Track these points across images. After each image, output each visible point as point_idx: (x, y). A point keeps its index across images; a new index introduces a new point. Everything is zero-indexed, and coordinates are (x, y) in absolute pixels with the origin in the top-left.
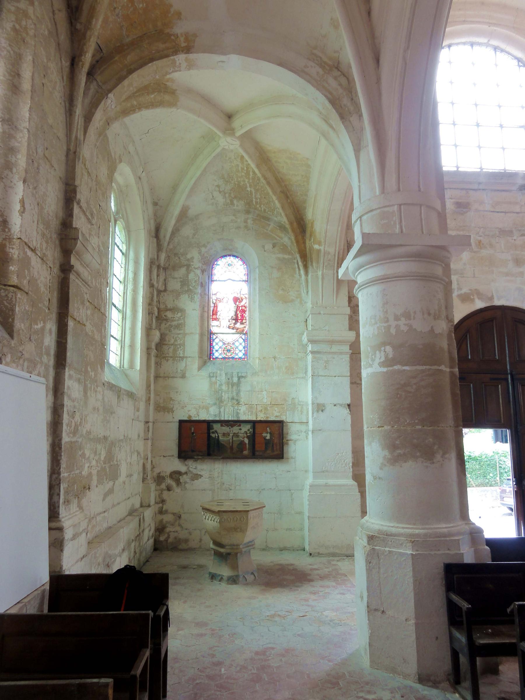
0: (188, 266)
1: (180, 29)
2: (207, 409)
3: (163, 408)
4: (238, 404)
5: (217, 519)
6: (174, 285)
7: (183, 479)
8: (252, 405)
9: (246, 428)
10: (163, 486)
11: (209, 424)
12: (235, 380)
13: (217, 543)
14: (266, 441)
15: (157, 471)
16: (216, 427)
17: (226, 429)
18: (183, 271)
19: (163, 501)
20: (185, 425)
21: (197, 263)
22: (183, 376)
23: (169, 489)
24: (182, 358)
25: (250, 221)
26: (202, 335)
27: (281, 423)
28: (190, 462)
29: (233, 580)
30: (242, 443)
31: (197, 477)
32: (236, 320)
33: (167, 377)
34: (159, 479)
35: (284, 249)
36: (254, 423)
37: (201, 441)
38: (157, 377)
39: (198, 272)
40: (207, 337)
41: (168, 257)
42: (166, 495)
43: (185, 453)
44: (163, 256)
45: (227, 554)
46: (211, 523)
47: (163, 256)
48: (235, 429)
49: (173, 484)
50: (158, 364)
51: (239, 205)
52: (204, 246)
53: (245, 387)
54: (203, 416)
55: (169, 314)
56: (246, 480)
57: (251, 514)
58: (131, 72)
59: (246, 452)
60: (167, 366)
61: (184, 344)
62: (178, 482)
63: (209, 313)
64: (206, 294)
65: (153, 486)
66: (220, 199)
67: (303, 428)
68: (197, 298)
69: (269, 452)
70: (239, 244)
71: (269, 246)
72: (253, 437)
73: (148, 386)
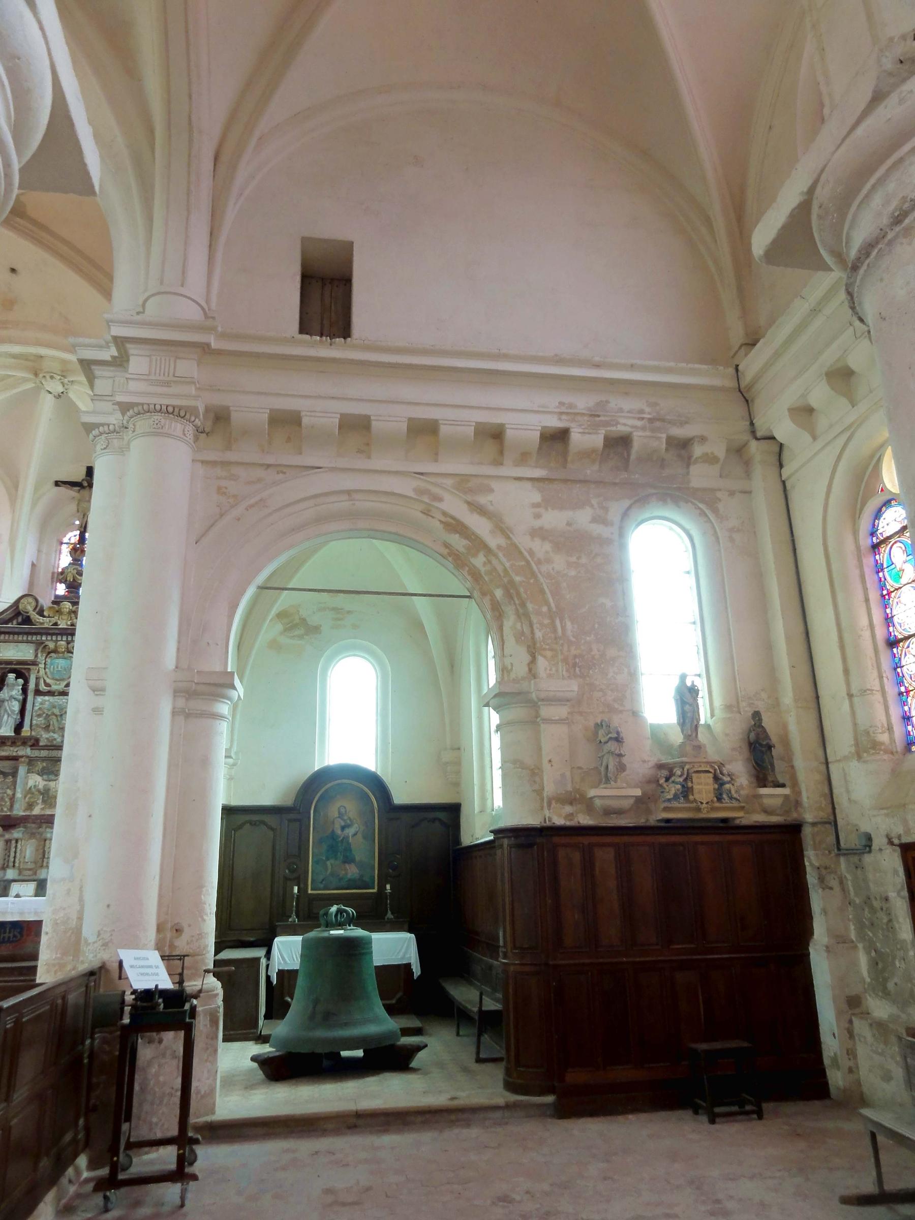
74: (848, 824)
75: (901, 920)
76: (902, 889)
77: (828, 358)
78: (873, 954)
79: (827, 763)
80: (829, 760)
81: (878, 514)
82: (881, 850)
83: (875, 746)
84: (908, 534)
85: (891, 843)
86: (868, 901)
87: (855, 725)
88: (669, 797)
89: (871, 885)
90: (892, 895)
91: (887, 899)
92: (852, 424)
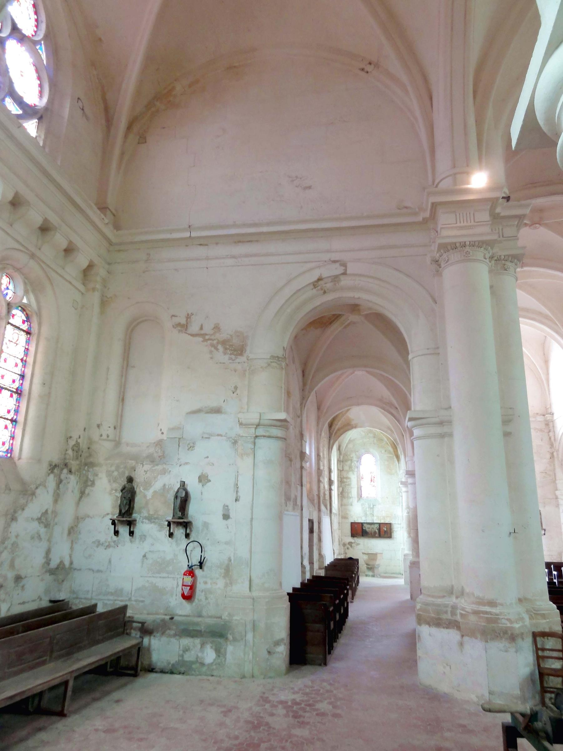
0: (351, 460)
1: (353, 423)
2: (361, 517)
3: (344, 517)
4: (373, 515)
5: (367, 556)
6: (346, 468)
7: (353, 545)
8: (378, 517)
9: (377, 526)
10: (346, 547)
11: (362, 524)
12: (372, 506)
13: (367, 564)
14: (384, 531)
15: (343, 541)
16: (365, 525)
17: (369, 526)
18: (349, 462)
19: (346, 553)
20: (353, 524)
21: (355, 459)
22: (352, 505)
23: (348, 548)
24: (351, 498)
25: (375, 441)
26: (358, 488)
27: (390, 524)
28: (355, 538)
29: (373, 576)
30: (375, 532)
31: (358, 544)
32: (371, 481)
33: (345, 505)
34: (344, 545)
35: (390, 453)
36: (380, 524)
37: (359, 530)
38: (341, 505)
39: (356, 462)
40: (360, 488)
41: (343, 457)
42: (347, 551)
43: (353, 535)
44: (342, 457)
45: (371, 568)
46: (366, 557)
47: (342, 457)
48: (372, 526)
49: (349, 547)
50: (342, 500)
51: (371, 435)
52: (358, 452)
53: (376, 509)
54: (360, 521)
55: (345, 480)
56: (377, 545)
57: (378, 555)
58: (341, 434)
59: (377, 535)
60: (345, 501)
61: (351, 492)
62: (351, 546)
63: (360, 478)
64: (358, 471)
65: (342, 547)
66: (363, 434)
67: (399, 526)
68: (355, 473)
69: (386, 535)
70: (371, 450)
71: (383, 451)
72: (379, 530)
73: (339, 509)
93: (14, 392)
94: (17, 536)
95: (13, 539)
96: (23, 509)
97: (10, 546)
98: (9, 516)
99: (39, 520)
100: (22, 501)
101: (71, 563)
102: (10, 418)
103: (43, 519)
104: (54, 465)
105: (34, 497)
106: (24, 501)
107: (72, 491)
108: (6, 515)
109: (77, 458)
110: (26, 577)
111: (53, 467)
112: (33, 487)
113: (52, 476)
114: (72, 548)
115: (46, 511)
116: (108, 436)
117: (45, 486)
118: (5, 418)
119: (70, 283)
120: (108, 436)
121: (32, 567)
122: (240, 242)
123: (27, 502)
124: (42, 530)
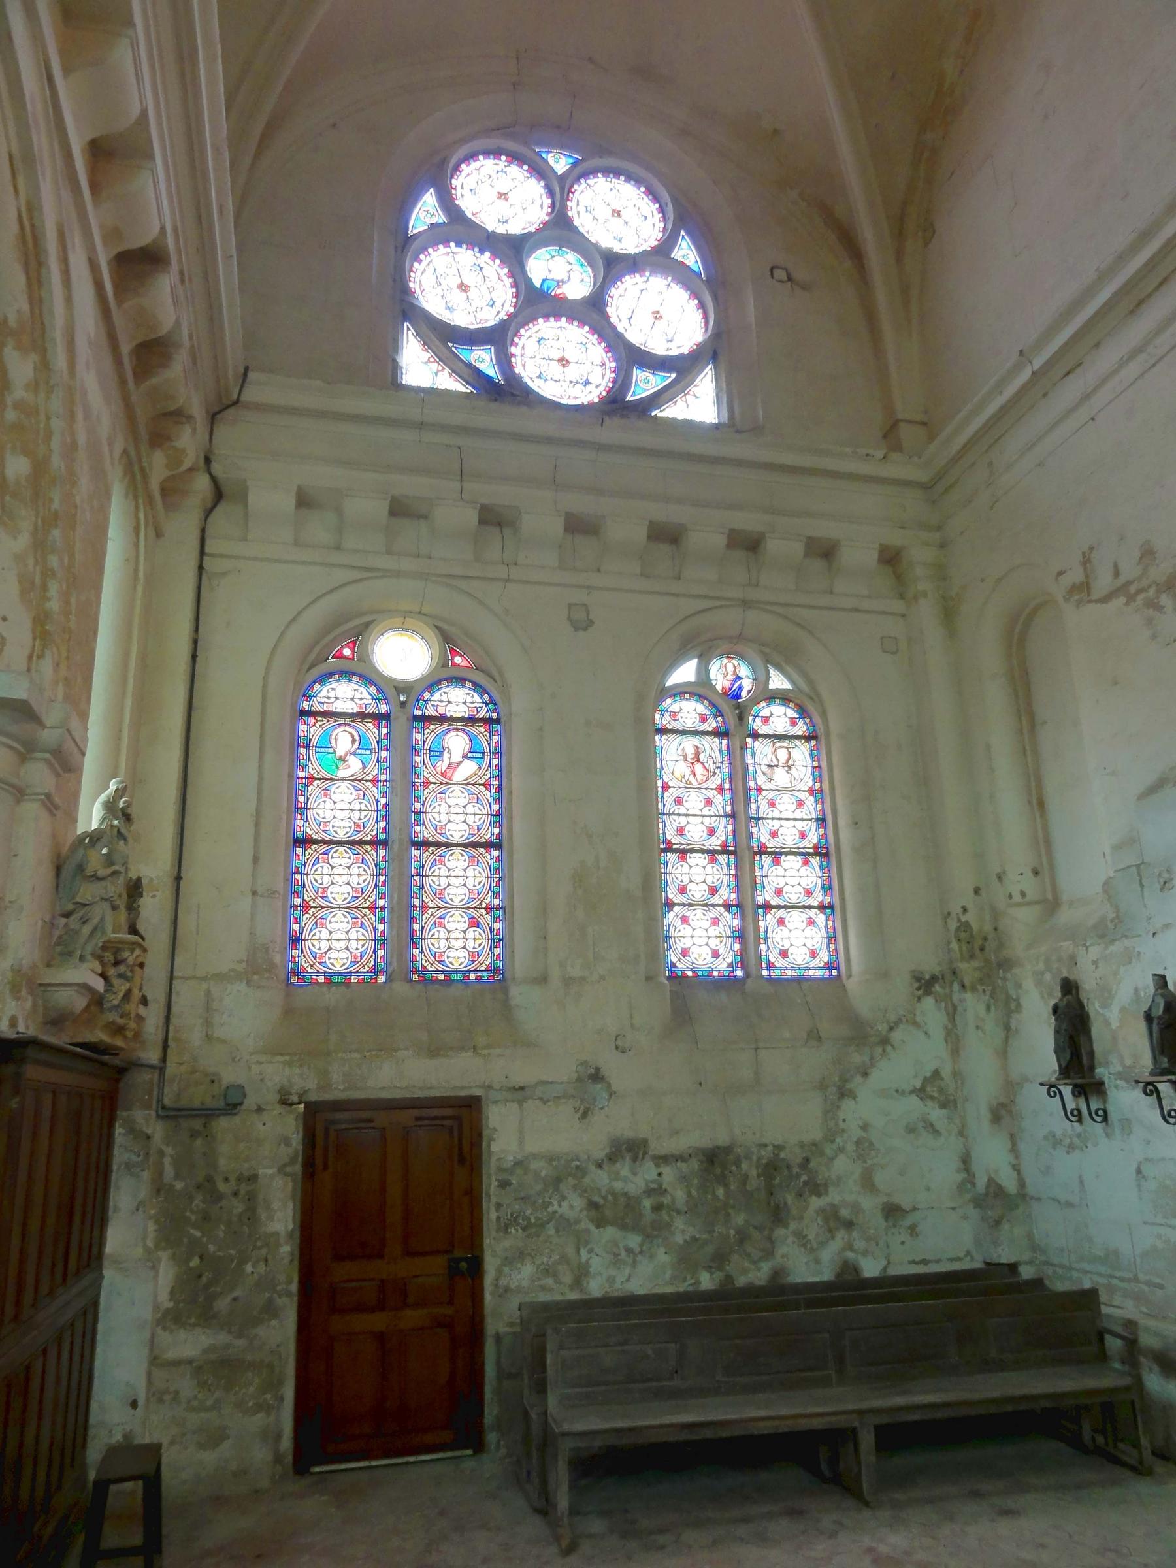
74: (194, 1072)
75: (276, 1205)
76: (293, 1161)
77: (411, 486)
78: (195, 1262)
79: (171, 978)
80: (175, 974)
81: (324, 678)
82: (259, 1110)
83: (272, 966)
84: (384, 731)
85: (285, 1102)
86: (207, 1186)
87: (252, 934)
88: (116, 1002)
89: (222, 1162)
90: (266, 1172)
91: (253, 1178)
92: (378, 570)
93: (809, 854)
94: (865, 1127)
95: (857, 1133)
96: (865, 1074)
97: (850, 1147)
98: (833, 1089)
99: (921, 1092)
100: (857, 1058)
101: (1022, 1184)
102: (816, 904)
103: (931, 1090)
104: (927, 977)
105: (889, 1048)
106: (866, 1059)
107: (977, 1027)
108: (822, 1086)
109: (972, 956)
110: (915, 1209)
111: (925, 984)
112: (882, 1028)
113: (929, 1002)
114: (1014, 1150)
115: (936, 1073)
116: (1023, 894)
117: (915, 1024)
118: (804, 907)
119: (856, 610)
120: (1023, 894)
121: (928, 1189)
122: (1141, 302)
123: (872, 1059)
124: (936, 1114)
